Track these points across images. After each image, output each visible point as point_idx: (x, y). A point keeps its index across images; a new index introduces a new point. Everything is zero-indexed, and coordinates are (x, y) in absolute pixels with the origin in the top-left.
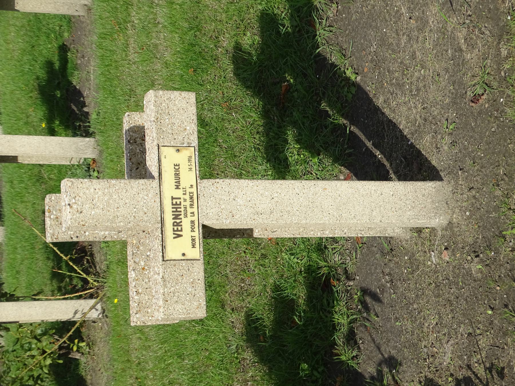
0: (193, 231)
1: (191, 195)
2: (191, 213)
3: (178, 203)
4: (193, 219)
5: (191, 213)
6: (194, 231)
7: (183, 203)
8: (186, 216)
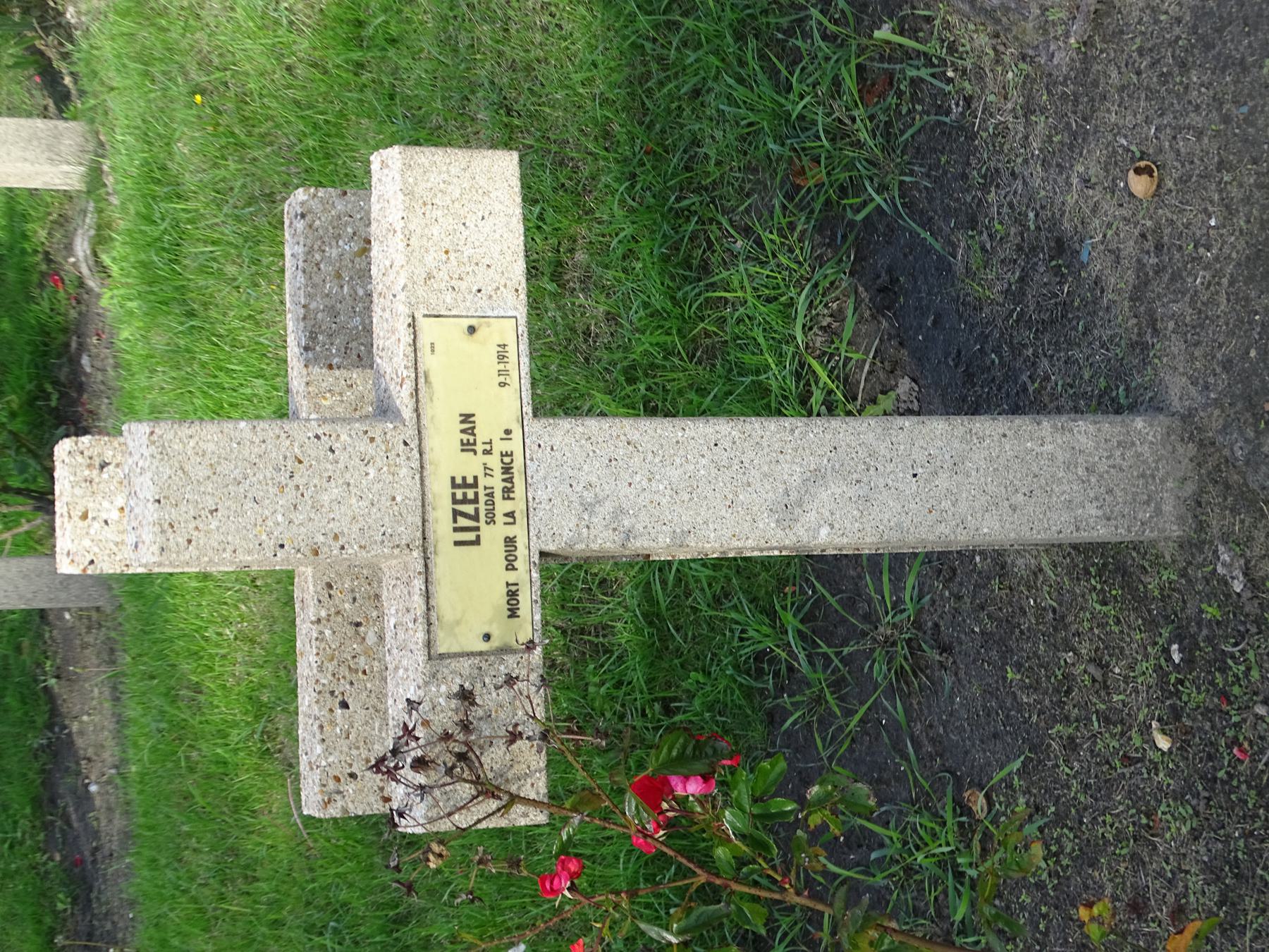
0: (510, 567)
1: (507, 460)
2: (506, 515)
3: (471, 495)
4: (510, 531)
5: (506, 515)
6: (514, 569)
7: (483, 482)
8: (491, 520)
